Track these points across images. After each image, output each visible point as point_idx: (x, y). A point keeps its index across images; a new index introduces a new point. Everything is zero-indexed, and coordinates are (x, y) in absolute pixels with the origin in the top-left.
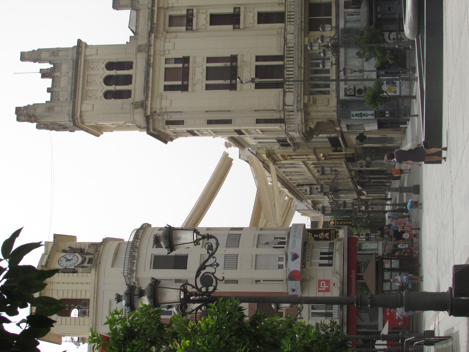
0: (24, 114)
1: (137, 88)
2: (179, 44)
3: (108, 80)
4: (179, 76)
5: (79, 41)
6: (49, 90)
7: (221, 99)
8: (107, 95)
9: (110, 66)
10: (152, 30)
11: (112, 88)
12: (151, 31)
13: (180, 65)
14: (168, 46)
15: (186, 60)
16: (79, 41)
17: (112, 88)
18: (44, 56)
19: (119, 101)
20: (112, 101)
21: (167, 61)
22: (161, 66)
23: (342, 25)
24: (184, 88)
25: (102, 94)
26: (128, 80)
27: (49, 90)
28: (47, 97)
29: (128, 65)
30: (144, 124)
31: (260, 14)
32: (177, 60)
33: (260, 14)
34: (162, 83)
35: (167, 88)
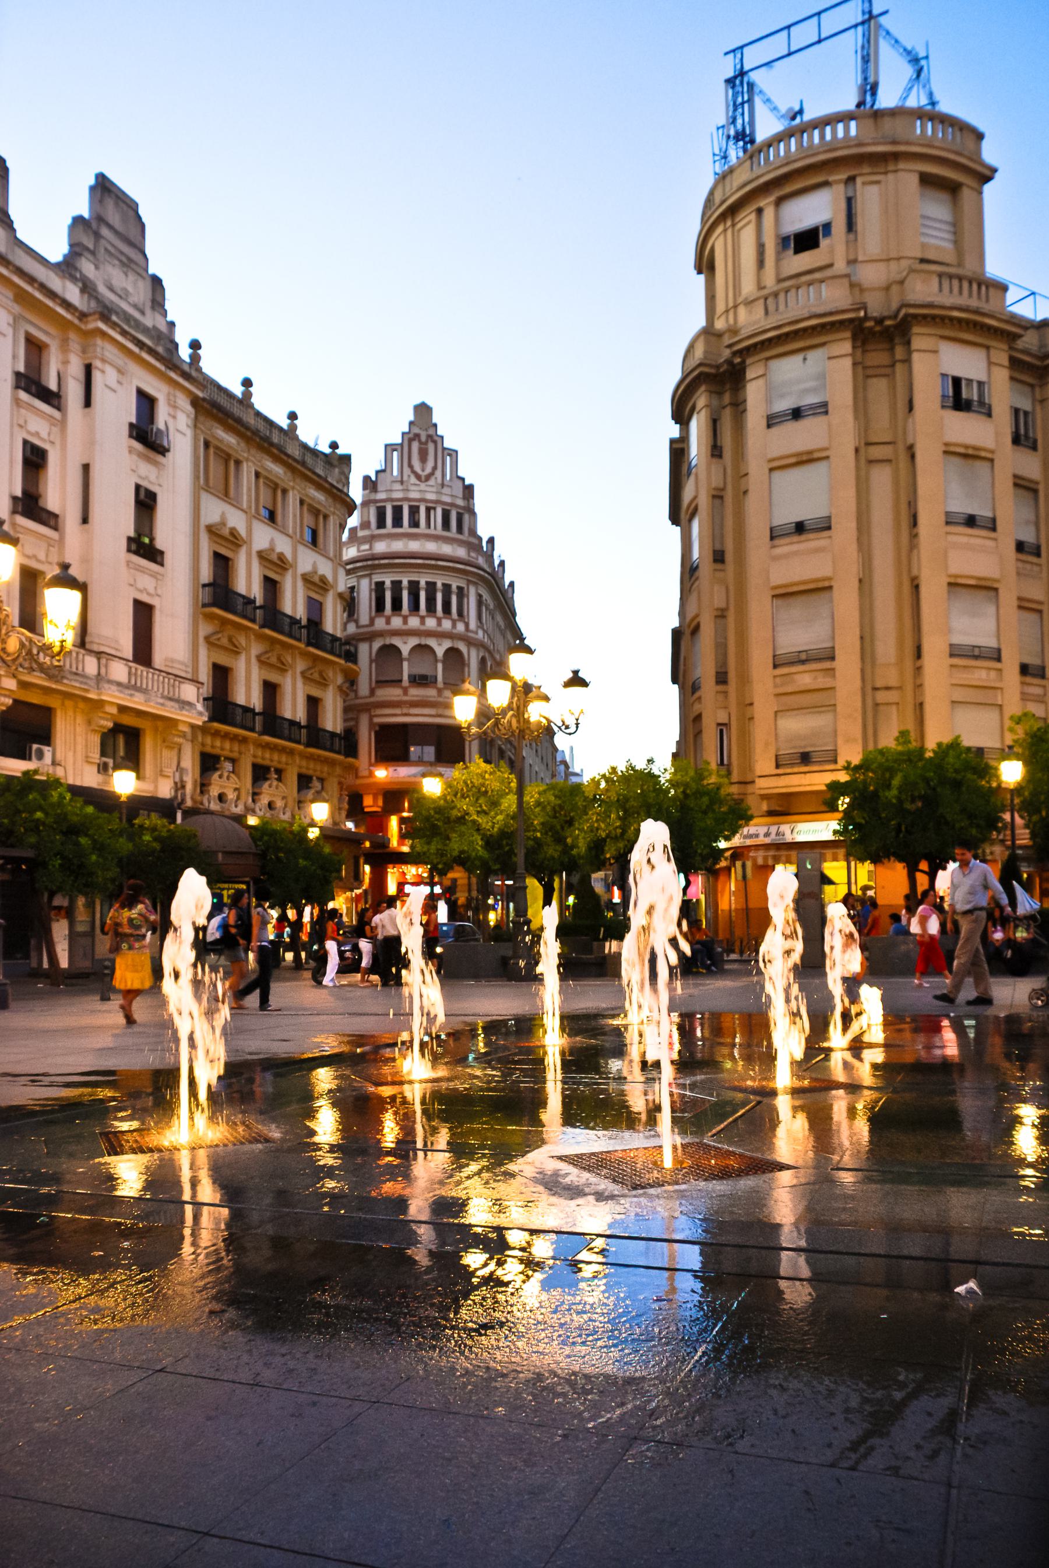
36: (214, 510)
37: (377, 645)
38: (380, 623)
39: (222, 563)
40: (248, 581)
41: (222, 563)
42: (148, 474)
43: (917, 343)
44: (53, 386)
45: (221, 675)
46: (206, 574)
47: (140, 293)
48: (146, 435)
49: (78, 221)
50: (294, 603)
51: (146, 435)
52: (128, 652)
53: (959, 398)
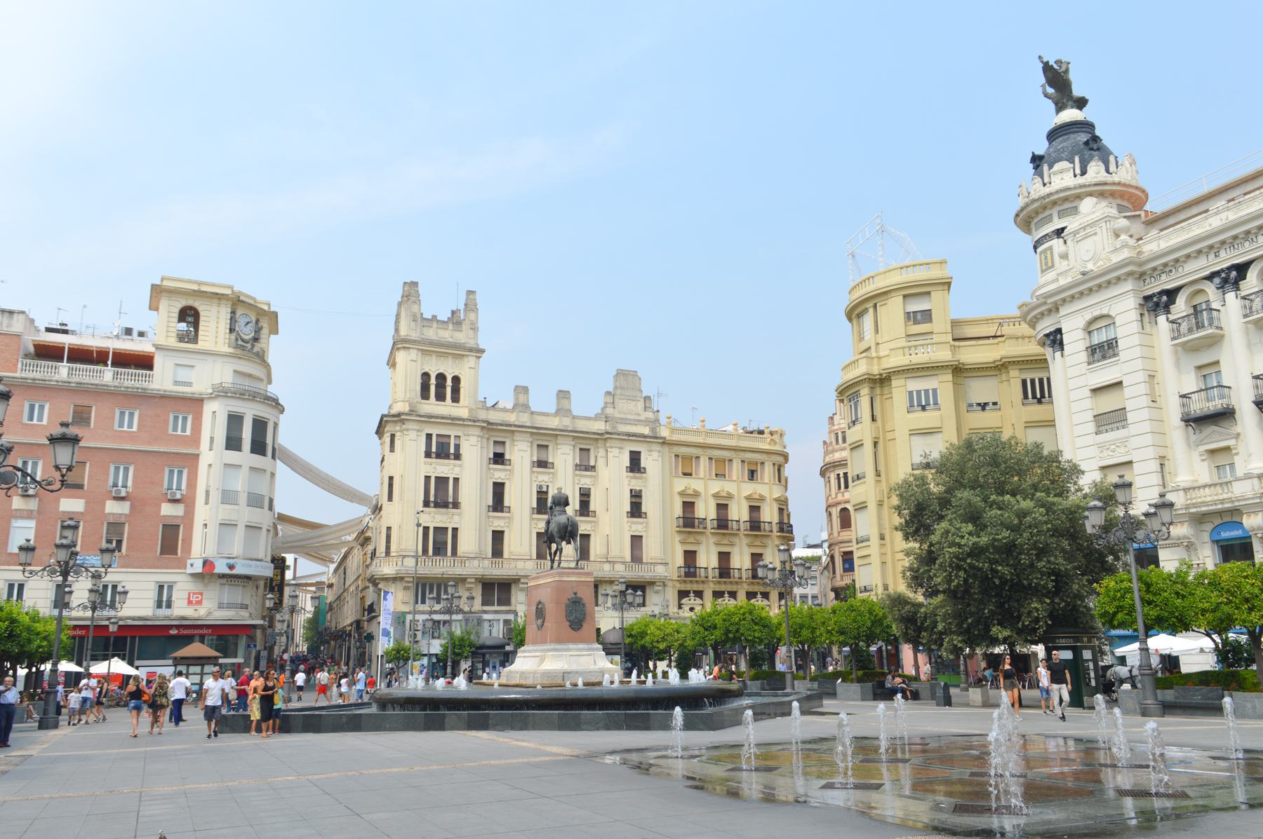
0: (411, 291)
1: (432, 406)
2: (474, 450)
3: (441, 377)
4: (442, 450)
5: (483, 351)
6: (434, 317)
7: (411, 491)
8: (426, 376)
9: (456, 380)
10: (489, 427)
11: (433, 381)
12: (489, 423)
13: (452, 451)
14: (474, 440)
15: (457, 456)
16: (483, 351)
17: (433, 381)
18: (472, 316)
19: (419, 388)
20: (419, 381)
21: (457, 437)
22: (452, 432)
23: (486, 617)
24: (428, 454)
25: (426, 370)
26: (440, 397)
27: (434, 317)
28: (427, 315)
29: (456, 398)
30: (393, 412)
31: (502, 532)
32: (457, 447)
33: (502, 532)
34: (435, 431)
35: (429, 436)
36: (681, 484)
37: (839, 508)
38: (840, 498)
39: (688, 506)
40: (706, 510)
41: (688, 506)
42: (636, 485)
43: (894, 383)
44: (592, 463)
45: (690, 556)
46: (678, 511)
47: (641, 405)
48: (635, 464)
49: (608, 393)
50: (739, 512)
51: (635, 464)
52: (628, 558)
53: (922, 403)
